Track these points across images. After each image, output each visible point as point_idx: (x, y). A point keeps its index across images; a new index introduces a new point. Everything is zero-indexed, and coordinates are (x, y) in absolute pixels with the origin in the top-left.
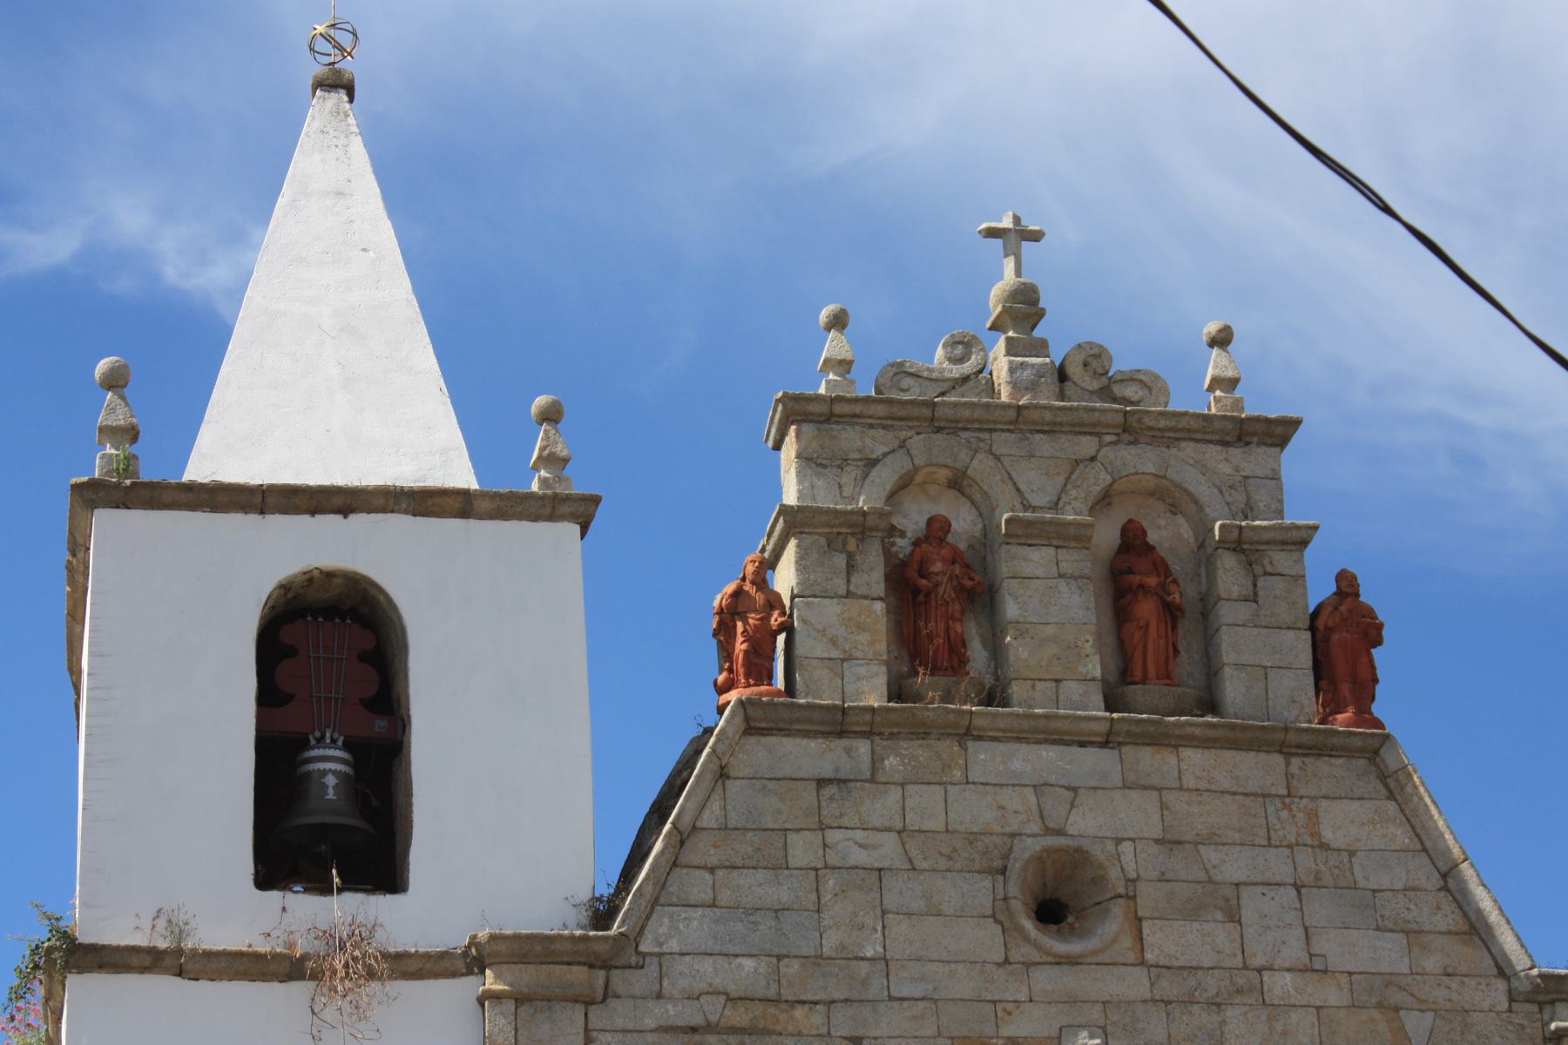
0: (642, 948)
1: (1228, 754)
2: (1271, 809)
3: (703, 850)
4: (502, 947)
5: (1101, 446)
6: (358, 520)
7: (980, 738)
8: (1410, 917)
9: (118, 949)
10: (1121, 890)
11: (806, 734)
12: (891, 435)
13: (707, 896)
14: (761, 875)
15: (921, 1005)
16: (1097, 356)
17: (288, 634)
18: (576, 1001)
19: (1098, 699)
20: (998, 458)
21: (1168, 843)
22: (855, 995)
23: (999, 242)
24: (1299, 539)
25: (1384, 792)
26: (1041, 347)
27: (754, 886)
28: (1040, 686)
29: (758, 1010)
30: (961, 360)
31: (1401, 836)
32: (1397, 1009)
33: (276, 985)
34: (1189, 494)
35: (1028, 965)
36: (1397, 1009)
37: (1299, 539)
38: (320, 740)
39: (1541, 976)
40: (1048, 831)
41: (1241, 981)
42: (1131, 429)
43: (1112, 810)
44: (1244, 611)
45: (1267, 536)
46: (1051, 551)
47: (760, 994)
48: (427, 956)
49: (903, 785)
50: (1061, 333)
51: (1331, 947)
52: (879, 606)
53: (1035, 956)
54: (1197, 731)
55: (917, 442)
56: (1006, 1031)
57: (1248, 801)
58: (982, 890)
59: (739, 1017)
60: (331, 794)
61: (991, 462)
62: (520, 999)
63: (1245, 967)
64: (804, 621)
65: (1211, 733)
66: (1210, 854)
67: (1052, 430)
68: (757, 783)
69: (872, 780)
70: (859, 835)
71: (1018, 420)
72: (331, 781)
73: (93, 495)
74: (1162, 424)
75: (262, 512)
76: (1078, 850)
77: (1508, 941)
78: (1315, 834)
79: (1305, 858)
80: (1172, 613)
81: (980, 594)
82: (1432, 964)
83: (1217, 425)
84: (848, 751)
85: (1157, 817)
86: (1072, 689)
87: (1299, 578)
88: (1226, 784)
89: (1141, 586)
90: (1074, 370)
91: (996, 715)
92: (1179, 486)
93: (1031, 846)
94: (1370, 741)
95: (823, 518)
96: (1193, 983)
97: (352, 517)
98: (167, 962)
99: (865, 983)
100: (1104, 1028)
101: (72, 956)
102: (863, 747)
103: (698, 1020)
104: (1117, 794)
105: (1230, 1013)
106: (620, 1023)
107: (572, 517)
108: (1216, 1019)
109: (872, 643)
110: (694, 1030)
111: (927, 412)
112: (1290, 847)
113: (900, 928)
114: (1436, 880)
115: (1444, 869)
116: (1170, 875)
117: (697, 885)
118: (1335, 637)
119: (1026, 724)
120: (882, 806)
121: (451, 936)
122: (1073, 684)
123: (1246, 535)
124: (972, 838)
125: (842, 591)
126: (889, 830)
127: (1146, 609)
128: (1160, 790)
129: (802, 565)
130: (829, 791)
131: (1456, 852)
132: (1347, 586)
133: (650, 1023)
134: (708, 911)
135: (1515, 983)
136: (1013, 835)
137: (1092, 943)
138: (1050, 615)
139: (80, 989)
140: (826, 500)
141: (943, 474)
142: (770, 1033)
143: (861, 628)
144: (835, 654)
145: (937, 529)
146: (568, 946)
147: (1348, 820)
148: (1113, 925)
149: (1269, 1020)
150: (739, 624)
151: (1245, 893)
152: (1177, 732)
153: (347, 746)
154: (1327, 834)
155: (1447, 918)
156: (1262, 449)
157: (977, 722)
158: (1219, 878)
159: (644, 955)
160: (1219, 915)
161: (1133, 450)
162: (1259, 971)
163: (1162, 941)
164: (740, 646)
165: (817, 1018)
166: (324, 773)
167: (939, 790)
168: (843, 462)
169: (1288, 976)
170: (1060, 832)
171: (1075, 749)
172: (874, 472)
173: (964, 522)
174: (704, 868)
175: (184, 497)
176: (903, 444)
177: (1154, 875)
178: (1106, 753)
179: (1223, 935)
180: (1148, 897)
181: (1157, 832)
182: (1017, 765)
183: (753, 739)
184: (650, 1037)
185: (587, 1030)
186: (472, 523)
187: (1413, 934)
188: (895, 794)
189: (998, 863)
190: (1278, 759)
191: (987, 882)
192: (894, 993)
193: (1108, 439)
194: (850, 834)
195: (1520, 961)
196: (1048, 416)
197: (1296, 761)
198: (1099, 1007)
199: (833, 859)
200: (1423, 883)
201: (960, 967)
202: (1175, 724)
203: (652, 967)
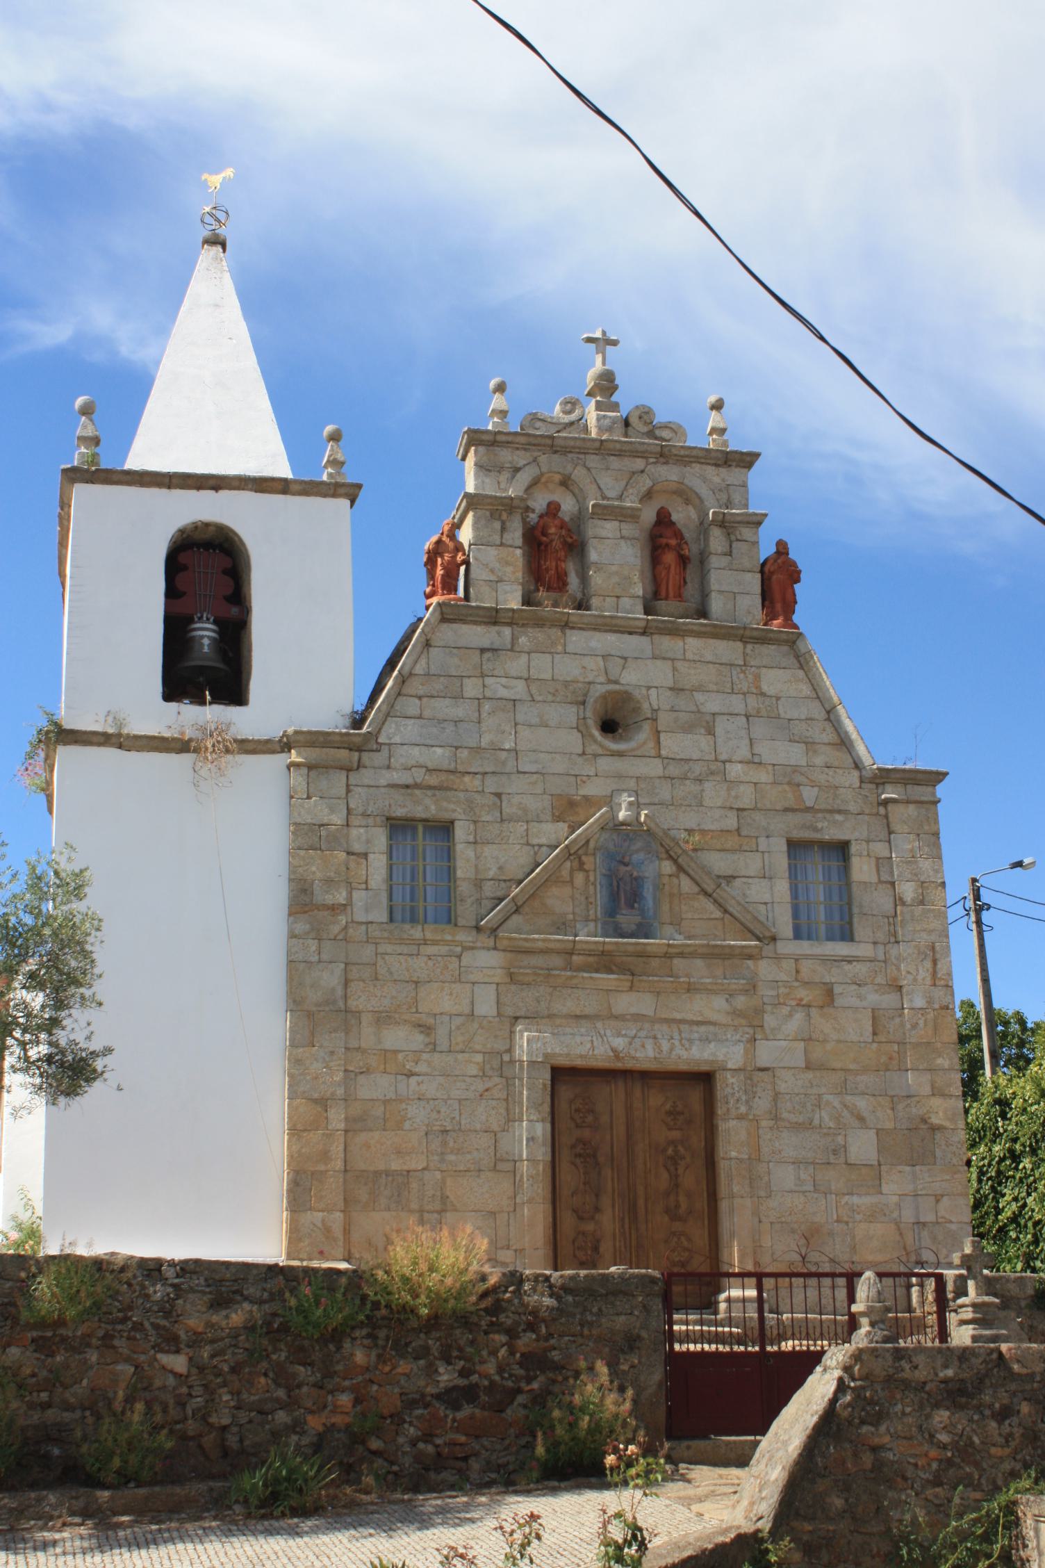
0: (380, 740)
1: (712, 641)
2: (734, 673)
3: (415, 686)
4: (300, 738)
5: (647, 464)
6: (224, 494)
7: (573, 628)
8: (808, 734)
9: (85, 733)
10: (649, 715)
11: (475, 623)
12: (528, 454)
13: (417, 712)
14: (447, 701)
15: (535, 776)
16: (647, 413)
17: (183, 558)
18: (341, 769)
19: (640, 608)
20: (589, 469)
21: (676, 690)
22: (498, 770)
23: (593, 346)
24: (756, 522)
25: (797, 665)
26: (615, 407)
27: (443, 707)
28: (608, 599)
29: (443, 777)
30: (570, 412)
31: (806, 690)
32: (798, 785)
33: (174, 755)
34: (696, 494)
35: (595, 756)
36: (798, 785)
37: (756, 522)
38: (200, 618)
39: (878, 769)
40: (610, 681)
41: (713, 767)
42: (665, 455)
43: (646, 671)
44: (724, 561)
45: (739, 519)
46: (617, 523)
47: (445, 767)
48: (259, 741)
49: (529, 653)
50: (626, 400)
51: (765, 751)
52: (519, 552)
53: (600, 751)
54: (695, 628)
55: (543, 459)
56: (581, 792)
57: (722, 668)
58: (570, 714)
59: (433, 780)
60: (206, 649)
61: (584, 471)
62: (310, 767)
63: (716, 760)
64: (476, 559)
65: (703, 629)
66: (699, 697)
67: (620, 454)
68: (447, 650)
69: (512, 650)
70: (504, 680)
71: (601, 448)
72: (206, 642)
73: (74, 475)
74: (682, 453)
75: (169, 488)
76: (626, 692)
77: (861, 749)
78: (758, 687)
79: (752, 701)
80: (684, 561)
81: (576, 547)
82: (819, 760)
83: (713, 455)
84: (499, 633)
85: (671, 675)
86: (626, 602)
87: (756, 543)
88: (709, 658)
89: (667, 545)
90: (634, 421)
91: (582, 616)
92: (691, 489)
93: (598, 690)
95: (489, 501)
96: (687, 768)
97: (221, 492)
98: (114, 740)
99: (504, 763)
100: (636, 792)
101: (62, 735)
102: (507, 631)
103: (410, 781)
104: (649, 662)
105: (707, 785)
106: (366, 782)
107: (346, 496)
108: (698, 788)
109: (514, 573)
110: (407, 787)
111: (549, 442)
112: (744, 694)
113: (524, 733)
114: (823, 715)
115: (828, 707)
116: (676, 708)
117: (412, 706)
118: (774, 577)
119: (599, 621)
120: (517, 665)
121: (272, 731)
122: (626, 599)
123: (728, 518)
124: (566, 684)
125: (498, 542)
126: (521, 678)
127: (669, 558)
128: (673, 660)
129: (476, 526)
130: (487, 655)
131: (835, 699)
132: (782, 549)
133: (383, 782)
134: (417, 721)
135: (864, 773)
136: (590, 683)
137: (632, 744)
138: (615, 559)
139: (65, 754)
140: (490, 491)
141: (557, 478)
142: (451, 789)
143: (507, 563)
144: (493, 578)
145: (553, 509)
146: (337, 738)
147: (778, 680)
148: (643, 735)
149: (729, 789)
150: (439, 560)
151: (718, 719)
153: (215, 622)
154: (765, 688)
155: (829, 736)
156: (737, 470)
157: (572, 619)
158: (704, 710)
159: (381, 744)
160: (703, 731)
161: (665, 467)
162: (724, 762)
163: (673, 744)
164: (439, 572)
165: (477, 782)
166: (202, 637)
167: (549, 657)
168: (501, 469)
169: (739, 766)
170: (616, 682)
171: (626, 636)
172: (519, 475)
173: (568, 506)
174: (416, 696)
176: (535, 460)
177: (668, 707)
178: (645, 640)
179: (704, 742)
180: (664, 719)
181: (670, 684)
182: (593, 644)
183: (445, 625)
184: (383, 790)
185: (348, 786)
186: (289, 497)
187: (809, 744)
188: (524, 658)
189: (580, 699)
190: (739, 644)
191: (574, 709)
192: (521, 769)
193: (652, 460)
194: (498, 680)
195: (867, 760)
196: (618, 446)
197: (749, 647)
198: (634, 780)
199: (488, 694)
200: (816, 716)
201: (557, 756)
202: (684, 624)
203: (385, 750)
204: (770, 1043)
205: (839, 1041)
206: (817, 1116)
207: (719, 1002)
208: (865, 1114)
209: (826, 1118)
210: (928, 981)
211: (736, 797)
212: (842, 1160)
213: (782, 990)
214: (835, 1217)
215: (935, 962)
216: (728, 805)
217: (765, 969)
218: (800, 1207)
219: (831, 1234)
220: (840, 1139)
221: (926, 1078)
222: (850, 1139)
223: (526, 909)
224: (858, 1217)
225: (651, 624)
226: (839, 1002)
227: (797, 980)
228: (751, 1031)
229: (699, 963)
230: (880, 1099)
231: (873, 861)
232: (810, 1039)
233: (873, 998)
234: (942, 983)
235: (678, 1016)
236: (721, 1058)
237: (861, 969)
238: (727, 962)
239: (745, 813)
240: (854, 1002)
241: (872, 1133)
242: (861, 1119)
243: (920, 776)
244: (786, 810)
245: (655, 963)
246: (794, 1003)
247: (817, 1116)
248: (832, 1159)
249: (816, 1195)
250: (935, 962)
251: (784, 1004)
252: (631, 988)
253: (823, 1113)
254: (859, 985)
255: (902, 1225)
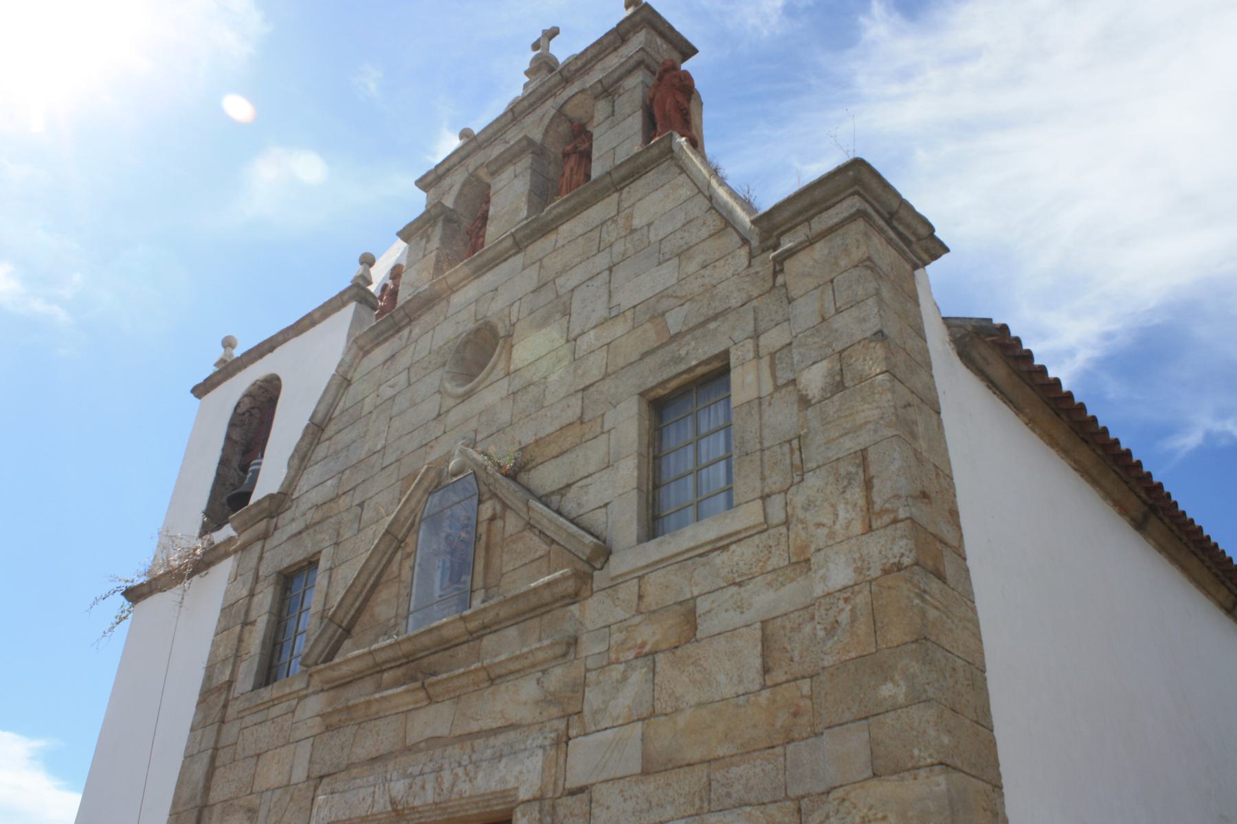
14: (346, 431)
54: (560, 210)
59: (317, 517)
65: (567, 206)
74: (580, 63)
82: (692, 267)
83: (605, 42)
91: (456, 271)
94: (662, 145)
133: (285, 537)
152: (550, 217)
175: (220, 377)
186: (319, 327)
204: (591, 737)
205: (700, 705)
207: (528, 689)
210: (857, 527)
211: (584, 374)
213: (617, 637)
215: (868, 485)
216: (572, 390)
217: (595, 612)
221: (855, 741)
223: (357, 628)
225: (518, 236)
226: (704, 628)
227: (639, 612)
228: (560, 724)
229: (512, 632)
230: (772, 809)
231: (765, 362)
232: (653, 714)
233: (764, 599)
234: (886, 519)
235: (475, 727)
236: (511, 784)
237: (742, 554)
238: (547, 618)
239: (592, 389)
240: (733, 618)
243: (818, 194)
244: (645, 355)
245: (462, 652)
246: (630, 655)
250: (868, 485)
251: (618, 662)
252: (429, 698)
254: (740, 584)
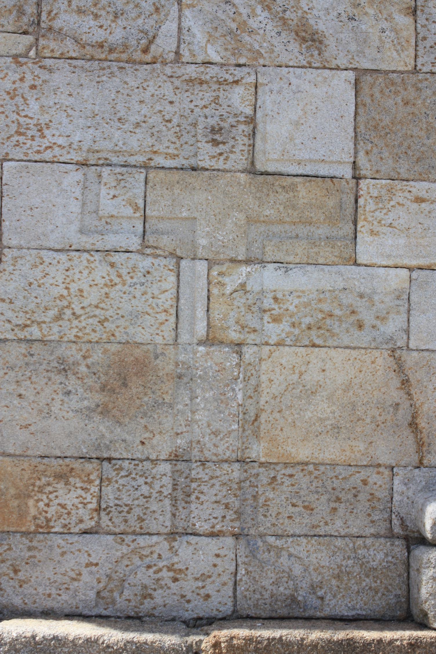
206: (170, 27)
208: (323, 25)
209: (199, 35)
212: (238, 159)
214: (201, 329)
218: (93, 296)
219: (181, 377)
220: (238, 99)
222: (266, 100)
224: (274, 331)
241: (342, 84)
242: (310, 39)
247: (170, 27)
248: (206, 153)
249: (146, 263)
253: (190, 19)
255: (411, 359)
